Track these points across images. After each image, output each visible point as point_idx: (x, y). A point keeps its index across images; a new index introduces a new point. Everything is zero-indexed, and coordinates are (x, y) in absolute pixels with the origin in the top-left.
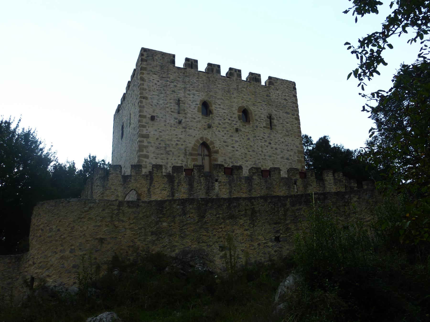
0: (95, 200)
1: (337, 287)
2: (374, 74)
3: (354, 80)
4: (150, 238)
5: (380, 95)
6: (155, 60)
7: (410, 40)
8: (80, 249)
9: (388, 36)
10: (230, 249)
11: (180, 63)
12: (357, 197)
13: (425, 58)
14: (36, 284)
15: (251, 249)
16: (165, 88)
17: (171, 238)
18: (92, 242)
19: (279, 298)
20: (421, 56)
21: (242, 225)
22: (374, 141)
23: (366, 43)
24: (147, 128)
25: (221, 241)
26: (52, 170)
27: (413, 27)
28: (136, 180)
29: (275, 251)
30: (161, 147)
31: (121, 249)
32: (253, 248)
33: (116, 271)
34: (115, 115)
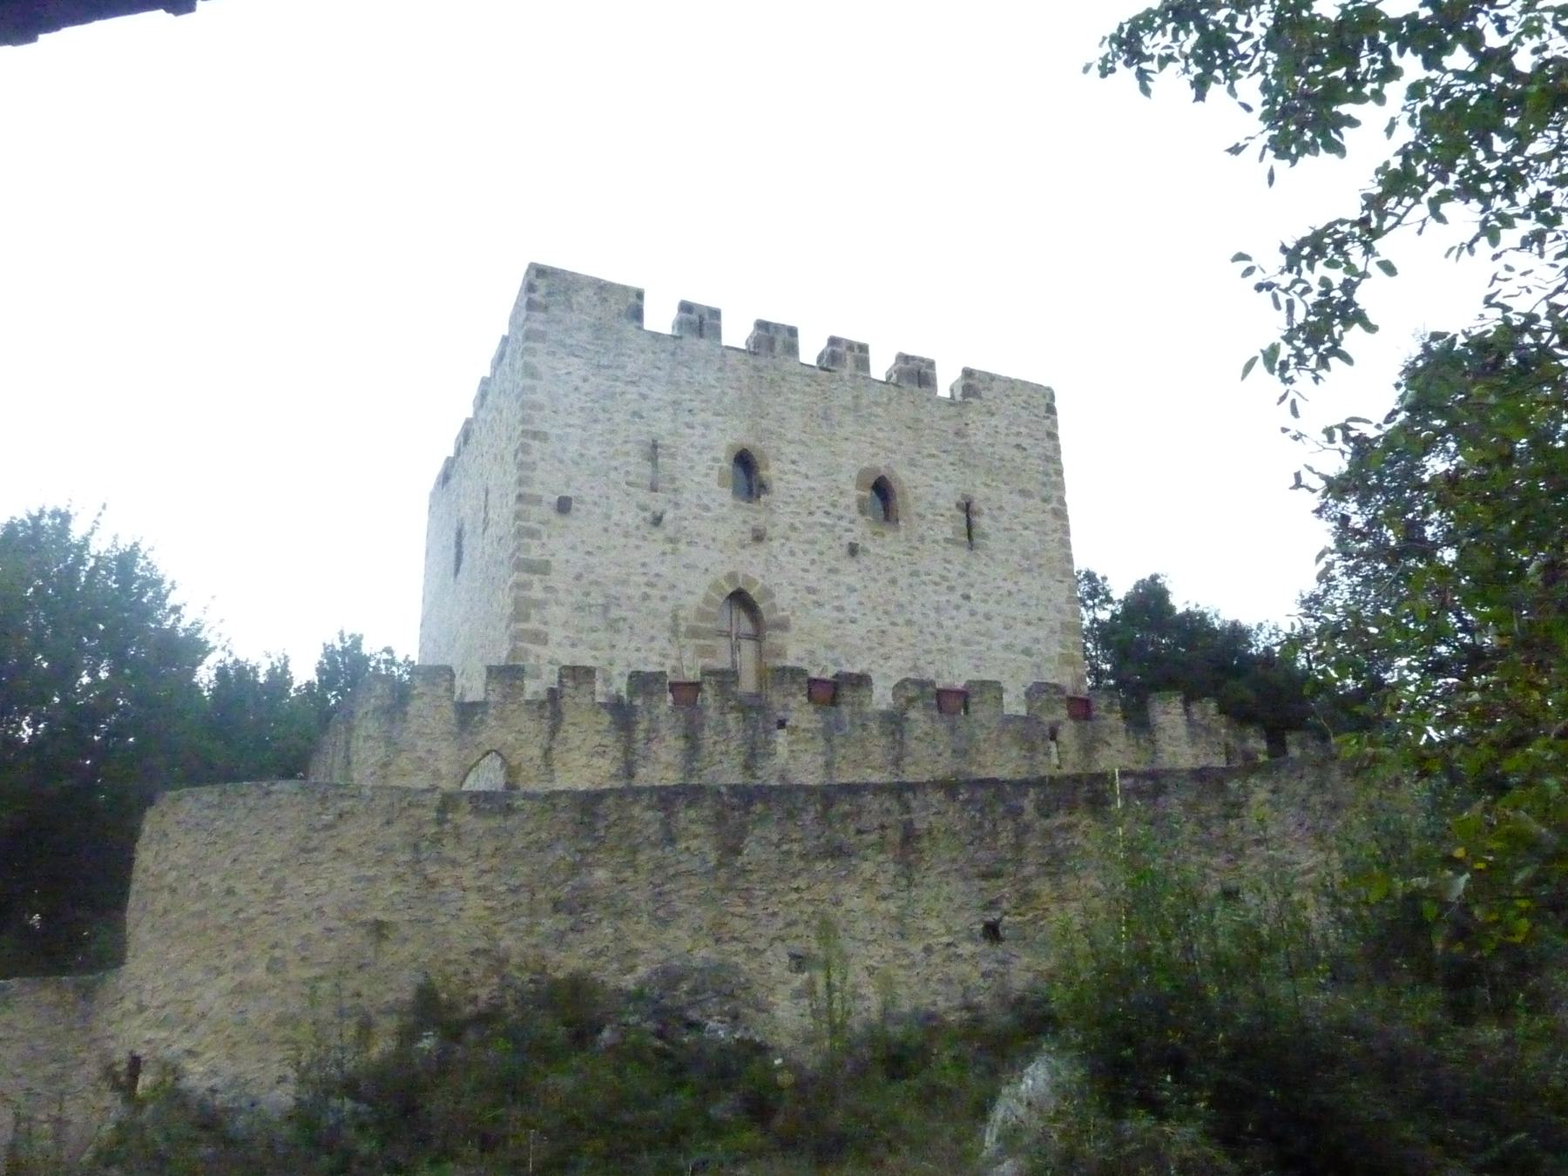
0: (360, 787)
1: (1202, 1105)
2: (1334, 361)
3: (1266, 382)
4: (548, 924)
5: (1353, 434)
6: (575, 306)
7: (1453, 248)
8: (303, 959)
9: (1377, 233)
10: (827, 966)
11: (660, 317)
12: (1269, 786)
13: (1506, 309)
14: (145, 1080)
15: (901, 966)
16: (608, 403)
17: (621, 924)
18: (347, 934)
19: (998, 1139)
20: (1493, 301)
21: (871, 882)
22: (1326, 592)
23: (1304, 257)
24: (545, 539)
25: (797, 937)
26: (210, 681)
27: (1467, 202)
28: (502, 718)
29: (985, 975)
30: (590, 606)
31: (448, 962)
32: (906, 962)
33: (427, 1037)
34: (433, 495)
